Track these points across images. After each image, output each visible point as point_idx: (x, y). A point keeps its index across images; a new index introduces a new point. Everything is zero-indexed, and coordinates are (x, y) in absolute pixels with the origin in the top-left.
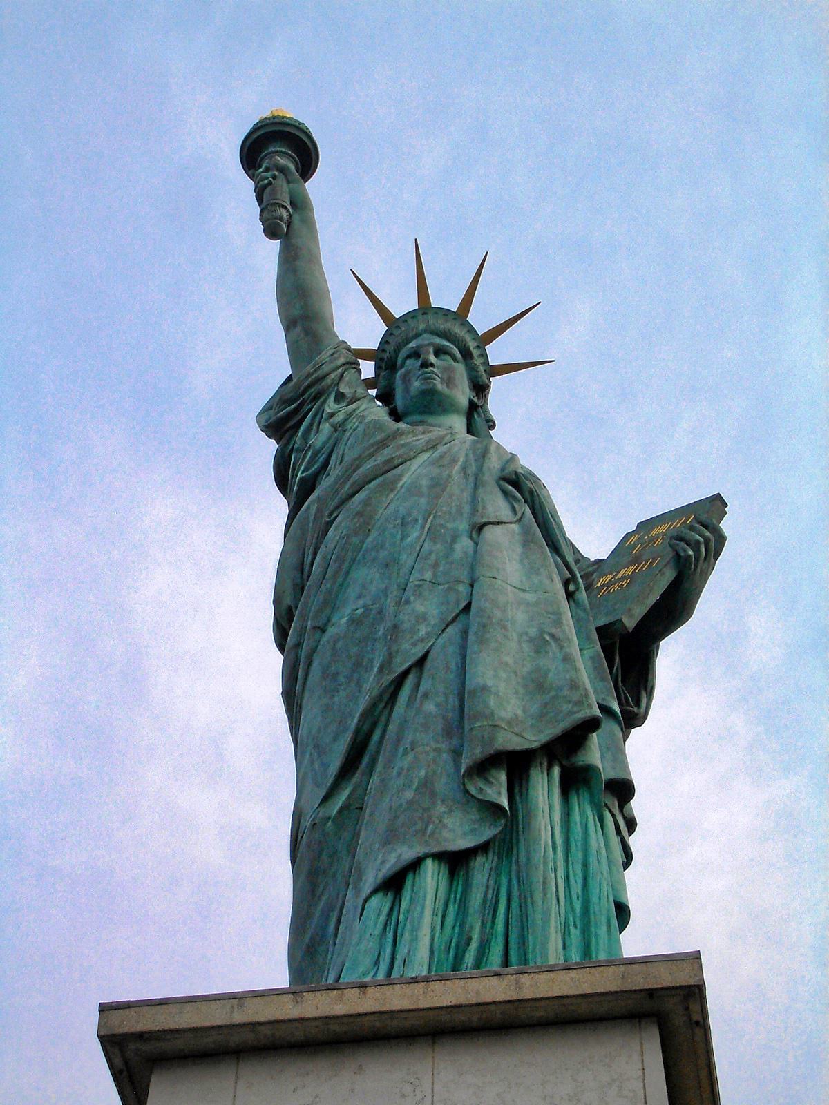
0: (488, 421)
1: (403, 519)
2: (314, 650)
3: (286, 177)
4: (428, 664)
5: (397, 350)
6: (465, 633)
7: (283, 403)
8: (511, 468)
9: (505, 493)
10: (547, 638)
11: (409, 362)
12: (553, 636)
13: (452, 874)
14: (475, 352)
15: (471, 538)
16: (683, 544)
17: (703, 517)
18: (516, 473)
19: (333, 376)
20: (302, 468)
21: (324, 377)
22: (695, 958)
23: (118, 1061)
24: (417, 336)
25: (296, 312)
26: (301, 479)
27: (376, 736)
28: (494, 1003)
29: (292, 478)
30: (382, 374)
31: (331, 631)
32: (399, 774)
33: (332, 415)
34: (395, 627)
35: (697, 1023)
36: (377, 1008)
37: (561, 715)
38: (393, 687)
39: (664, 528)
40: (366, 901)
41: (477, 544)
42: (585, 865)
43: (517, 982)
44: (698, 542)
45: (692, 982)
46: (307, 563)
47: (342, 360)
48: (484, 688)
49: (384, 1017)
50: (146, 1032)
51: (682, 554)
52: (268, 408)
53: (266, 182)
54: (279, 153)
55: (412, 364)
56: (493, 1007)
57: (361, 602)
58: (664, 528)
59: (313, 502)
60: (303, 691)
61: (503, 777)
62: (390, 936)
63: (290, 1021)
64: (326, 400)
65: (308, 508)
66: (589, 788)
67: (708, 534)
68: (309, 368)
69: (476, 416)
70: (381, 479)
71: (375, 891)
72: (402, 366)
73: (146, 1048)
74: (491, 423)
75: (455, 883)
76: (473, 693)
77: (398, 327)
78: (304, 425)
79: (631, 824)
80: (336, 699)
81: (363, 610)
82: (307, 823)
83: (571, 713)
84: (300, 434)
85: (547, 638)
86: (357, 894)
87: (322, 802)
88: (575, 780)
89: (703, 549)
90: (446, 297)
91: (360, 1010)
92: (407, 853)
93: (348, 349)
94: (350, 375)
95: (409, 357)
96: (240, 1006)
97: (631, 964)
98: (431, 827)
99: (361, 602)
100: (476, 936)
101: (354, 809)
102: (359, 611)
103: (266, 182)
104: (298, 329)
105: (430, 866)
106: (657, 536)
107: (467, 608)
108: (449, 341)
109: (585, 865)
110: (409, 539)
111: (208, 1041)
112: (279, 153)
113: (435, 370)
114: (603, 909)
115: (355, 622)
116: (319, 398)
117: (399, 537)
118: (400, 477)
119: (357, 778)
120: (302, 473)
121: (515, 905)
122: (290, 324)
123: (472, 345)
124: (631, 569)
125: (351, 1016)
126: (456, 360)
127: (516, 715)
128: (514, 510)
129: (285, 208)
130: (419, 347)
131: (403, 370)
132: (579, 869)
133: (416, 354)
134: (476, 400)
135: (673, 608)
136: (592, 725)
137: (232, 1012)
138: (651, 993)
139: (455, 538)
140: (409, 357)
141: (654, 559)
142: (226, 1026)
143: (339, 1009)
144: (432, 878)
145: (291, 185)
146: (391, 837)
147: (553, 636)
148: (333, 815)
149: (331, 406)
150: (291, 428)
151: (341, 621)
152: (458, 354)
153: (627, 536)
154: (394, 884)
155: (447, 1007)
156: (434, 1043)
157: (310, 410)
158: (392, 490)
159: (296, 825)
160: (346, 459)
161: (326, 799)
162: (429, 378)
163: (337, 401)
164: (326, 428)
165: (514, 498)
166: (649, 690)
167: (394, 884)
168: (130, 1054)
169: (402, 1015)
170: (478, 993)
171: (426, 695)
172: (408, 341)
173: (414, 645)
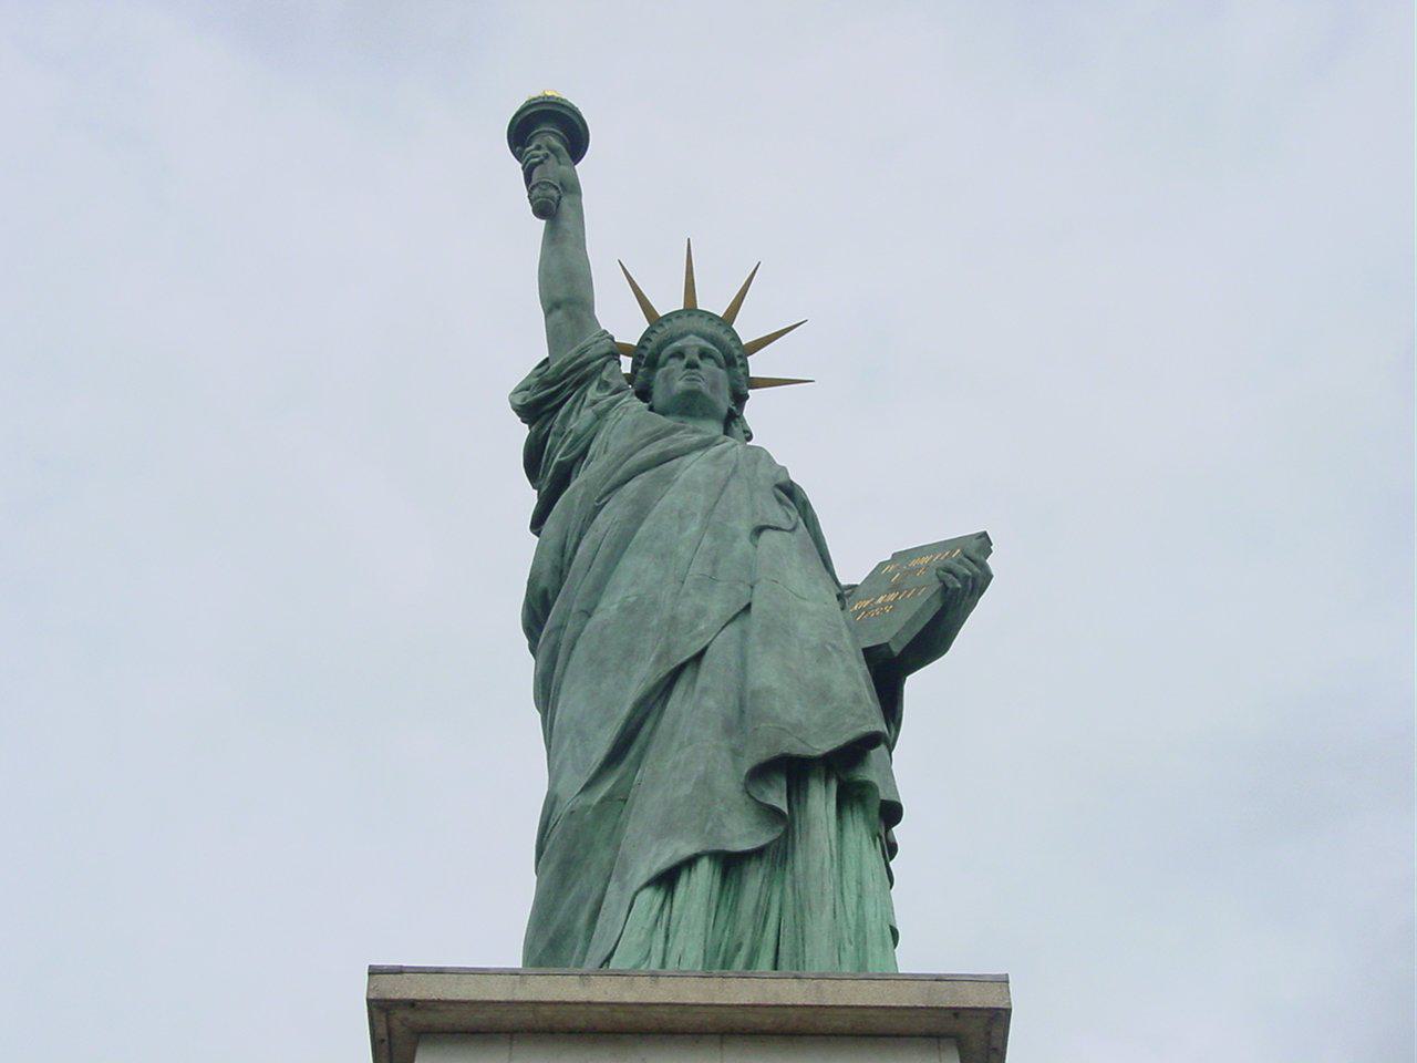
0: (745, 432)
1: (680, 512)
2: (577, 636)
3: (557, 157)
5: (660, 348)
6: (744, 634)
7: (544, 384)
8: (782, 480)
9: (780, 501)
10: (829, 648)
11: (671, 361)
12: (834, 647)
13: (725, 876)
14: (739, 362)
15: (751, 541)
16: (950, 576)
17: (972, 553)
18: (792, 482)
19: (597, 363)
20: (560, 453)
21: (587, 363)
23: (382, 1030)
24: (683, 335)
25: (560, 294)
26: (559, 463)
27: (647, 727)
28: (793, 1006)
29: (547, 460)
30: (641, 370)
31: (597, 618)
32: (675, 767)
33: (595, 403)
34: (673, 618)
35: (995, 1049)
36: (670, 1000)
37: (846, 726)
38: (668, 679)
39: (926, 560)
40: (636, 893)
41: (756, 546)
42: (860, 883)
43: (818, 987)
44: (967, 577)
45: (1001, 1005)
46: (570, 546)
47: (606, 349)
48: (769, 690)
49: (676, 1009)
50: (420, 1001)
51: (947, 592)
52: (523, 388)
53: (537, 160)
54: (548, 135)
55: (676, 365)
56: (791, 1011)
57: (633, 590)
58: (926, 560)
59: (580, 485)
60: (563, 675)
61: (784, 783)
62: (661, 932)
63: (577, 1003)
64: (588, 387)
65: (574, 490)
66: (864, 806)
67: (976, 569)
68: (573, 352)
69: (733, 425)
70: (653, 472)
71: (648, 885)
72: (664, 365)
73: (420, 1018)
74: (748, 435)
75: (727, 886)
76: (755, 694)
77: (661, 325)
78: (562, 412)
79: (891, 849)
80: (604, 685)
81: (635, 598)
82: (562, 810)
83: (854, 726)
84: (558, 418)
85: (829, 648)
86: (622, 888)
87: (582, 790)
88: (853, 795)
89: (970, 583)
90: (713, 301)
91: (653, 1000)
92: (686, 849)
93: (612, 338)
94: (611, 366)
95: (672, 356)
97: (936, 980)
98: (709, 825)
99: (633, 590)
100: (747, 942)
101: (619, 801)
102: (631, 600)
103: (537, 160)
104: (559, 314)
105: (704, 868)
106: (918, 568)
107: (748, 607)
108: (715, 345)
109: (860, 883)
110: (688, 532)
111: (480, 1018)
112: (548, 135)
113: (702, 373)
114: (874, 926)
115: (622, 609)
116: (581, 385)
117: (676, 528)
118: (674, 471)
119: (622, 768)
120: (562, 456)
121: (788, 916)
122: (551, 306)
123: (737, 353)
124: (892, 597)
125: (641, 1004)
126: (720, 367)
127: (800, 721)
128: (789, 517)
129: (557, 189)
130: (684, 347)
131: (665, 369)
132: (853, 884)
133: (680, 354)
134: (734, 408)
135: (931, 641)
136: (872, 740)
137: (514, 989)
138: (957, 1012)
139: (735, 537)
140: (672, 356)
141: (919, 589)
142: (508, 1003)
143: (630, 997)
144: (704, 873)
145: (562, 167)
146: (667, 829)
147: (834, 647)
148: (594, 804)
149: (592, 392)
150: (550, 410)
151: (609, 607)
152: (723, 362)
153: (882, 565)
154: (666, 880)
155: (744, 1005)
156: (722, 1042)
157: (570, 396)
158: (668, 482)
159: (547, 813)
160: (611, 449)
161: (588, 787)
162: (693, 380)
163: (599, 388)
164: (587, 415)
165: (788, 506)
166: (897, 721)
167: (666, 880)
168: (396, 1023)
169: (695, 1010)
170: (776, 994)
171: (705, 690)
172: (672, 340)
173: (693, 639)
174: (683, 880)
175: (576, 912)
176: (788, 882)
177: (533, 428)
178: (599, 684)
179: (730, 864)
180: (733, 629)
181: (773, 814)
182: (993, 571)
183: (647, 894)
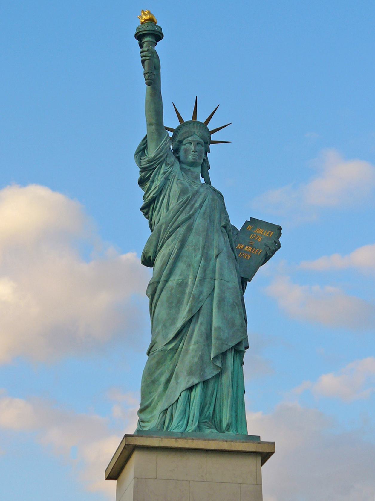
4: (202, 311)
10: (235, 304)
22: (274, 444)
27: (184, 331)
33: (165, 173)
62: (188, 404)
71: (185, 390)
72: (185, 145)
92: (196, 381)
96: (162, 440)
99: (181, 277)
102: (180, 281)
109: (237, 382)
154: (190, 389)
163: (166, 165)
167: (190, 389)
173: (199, 303)
174: (194, 390)
175: (161, 374)
176: (219, 384)
177: (143, 174)
178: (170, 310)
179: (205, 383)
180: (209, 299)
181: (218, 367)
182: (281, 245)
183: (185, 392)
